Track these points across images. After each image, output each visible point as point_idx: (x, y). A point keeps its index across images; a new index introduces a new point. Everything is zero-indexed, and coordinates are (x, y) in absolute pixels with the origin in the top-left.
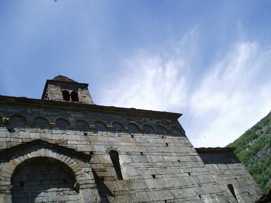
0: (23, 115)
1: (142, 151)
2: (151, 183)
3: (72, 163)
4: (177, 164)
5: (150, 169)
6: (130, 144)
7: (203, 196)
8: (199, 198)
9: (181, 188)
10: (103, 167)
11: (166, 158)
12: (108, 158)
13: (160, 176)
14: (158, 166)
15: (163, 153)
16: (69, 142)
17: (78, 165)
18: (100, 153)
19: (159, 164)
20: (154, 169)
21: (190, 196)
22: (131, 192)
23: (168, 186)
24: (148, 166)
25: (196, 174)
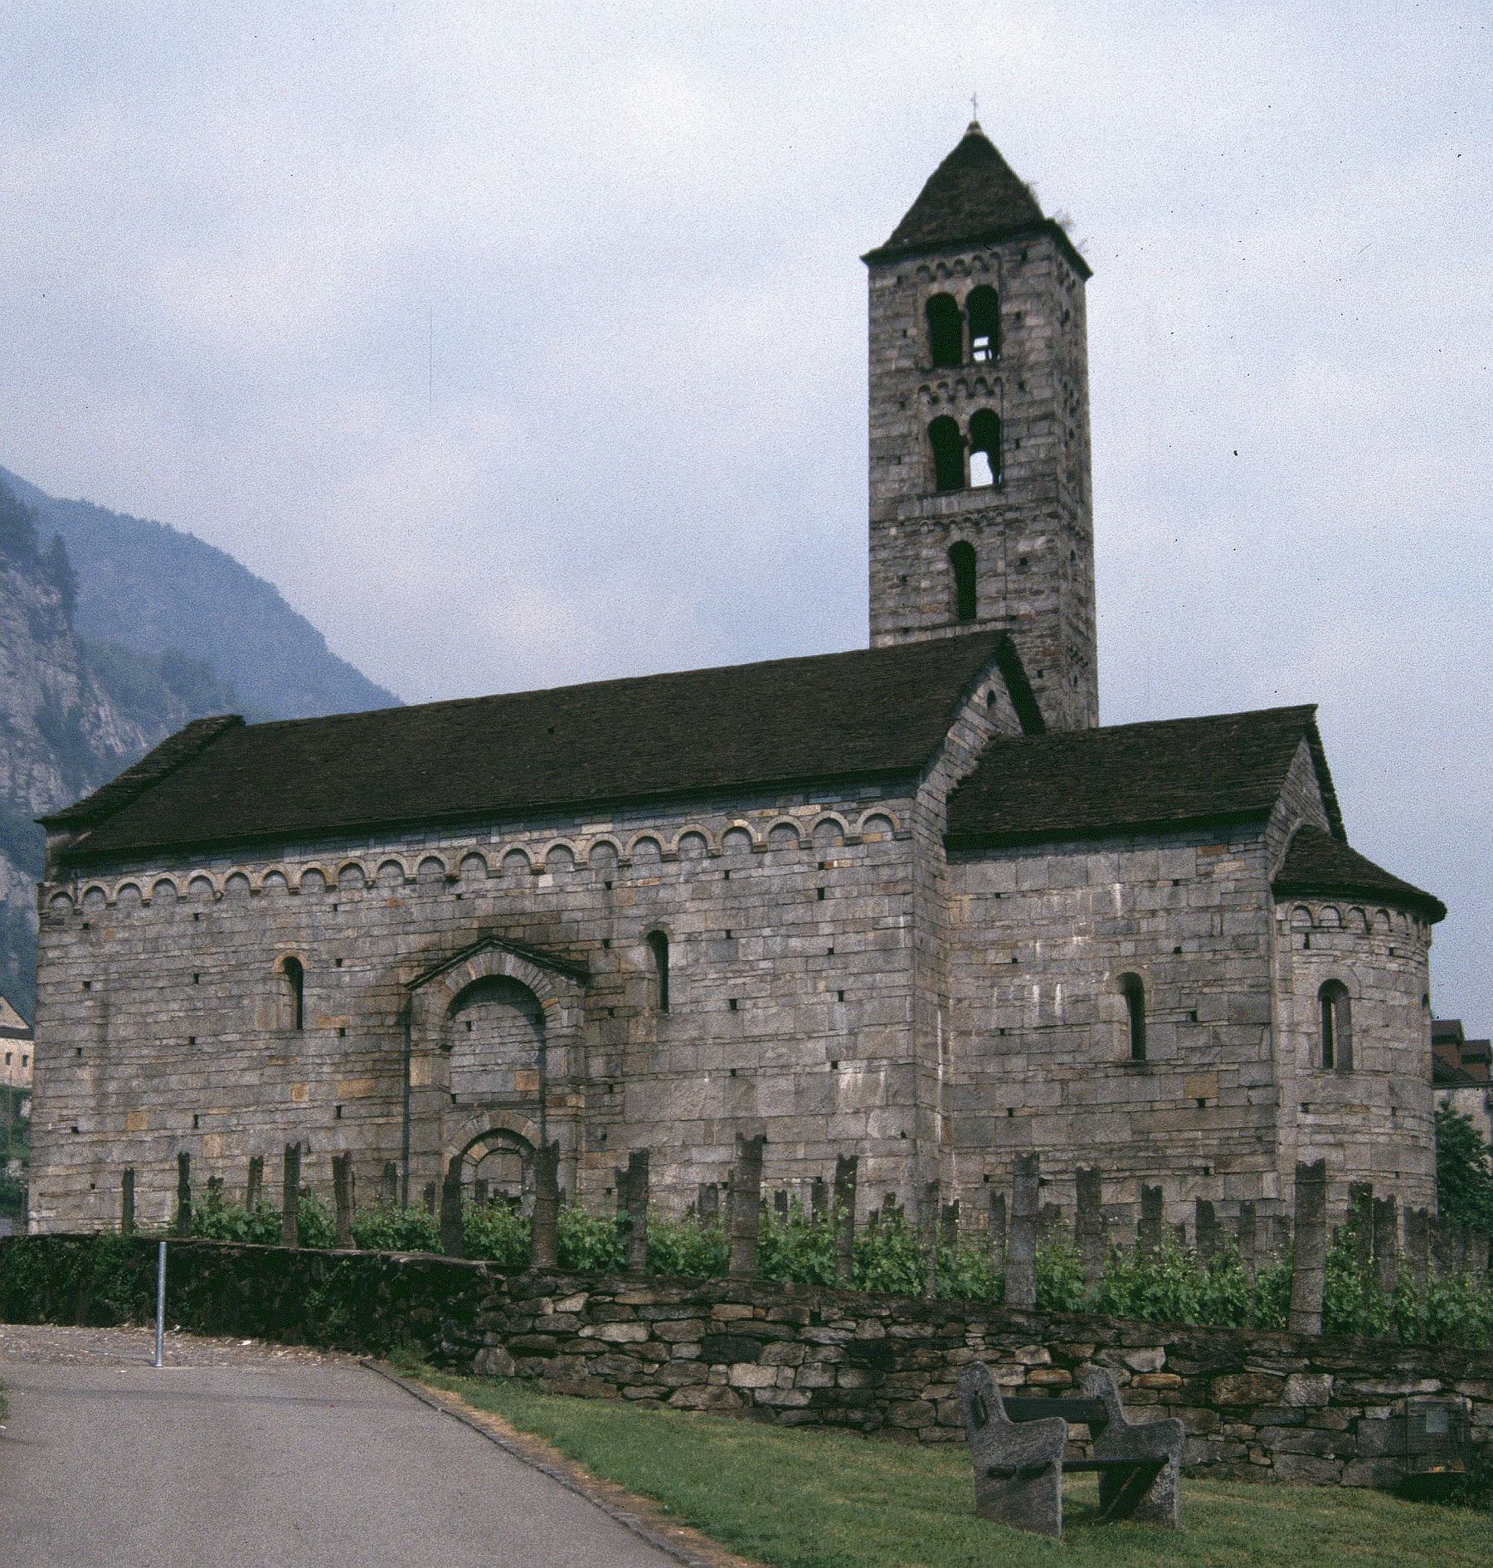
0: (483, 851)
1: (730, 925)
2: (719, 1022)
3: (543, 987)
4: (821, 963)
5: (731, 982)
6: (706, 905)
7: (842, 1065)
8: (827, 1067)
9: (792, 1038)
10: (620, 982)
11: (795, 943)
12: (639, 956)
13: (749, 1004)
14: (759, 972)
15: (790, 928)
16: (565, 916)
17: (553, 993)
18: (624, 942)
19: (763, 964)
20: (740, 981)
21: (808, 1060)
22: (660, 1048)
23: (756, 1032)
24: (729, 975)
25: (860, 994)
